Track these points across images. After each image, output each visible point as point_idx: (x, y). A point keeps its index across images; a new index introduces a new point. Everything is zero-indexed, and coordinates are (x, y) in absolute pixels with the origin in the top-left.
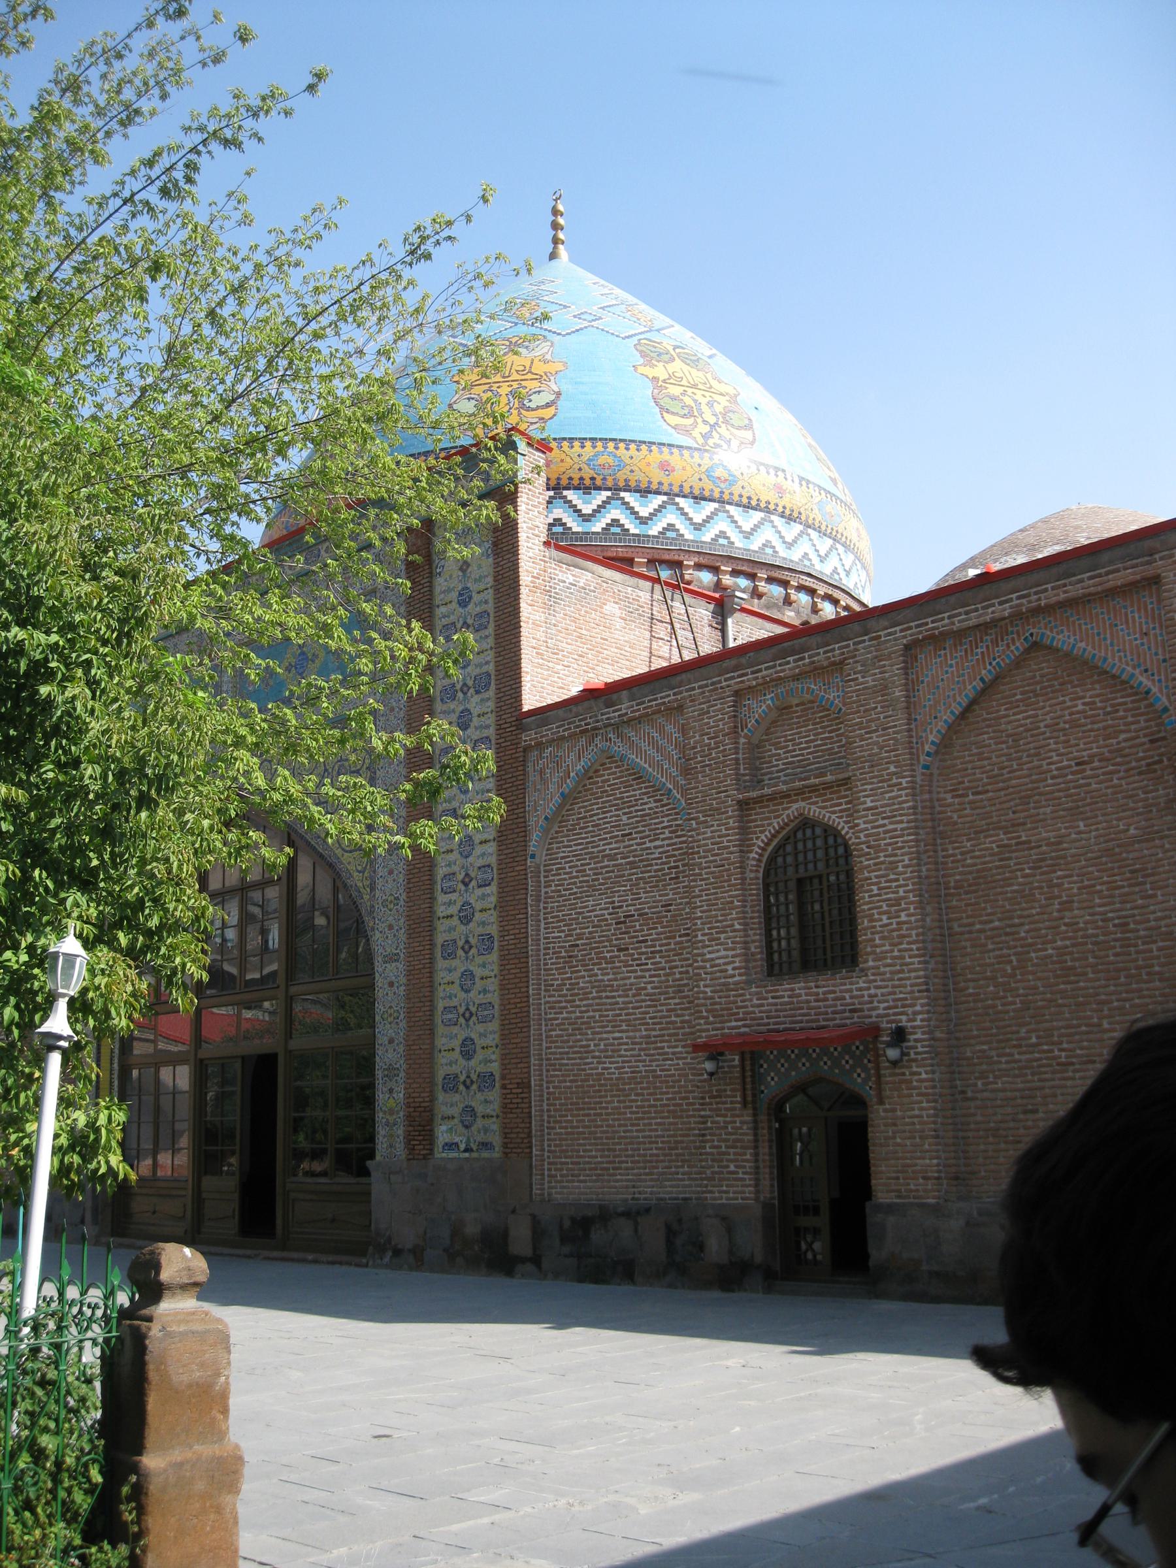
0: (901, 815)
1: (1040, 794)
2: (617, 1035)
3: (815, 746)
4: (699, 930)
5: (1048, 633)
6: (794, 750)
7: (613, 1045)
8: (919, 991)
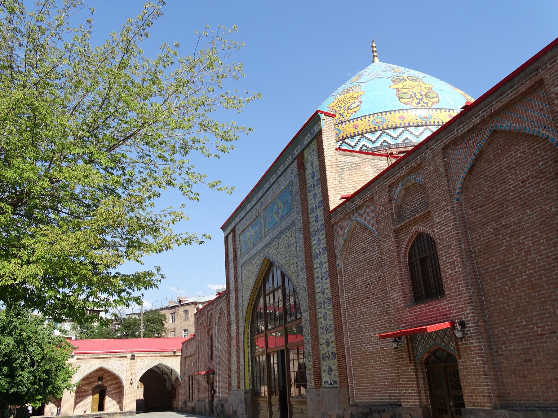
0: (450, 223)
1: (508, 201)
2: (370, 333)
3: (419, 202)
4: (387, 286)
5: (498, 124)
6: (413, 205)
7: (369, 338)
8: (467, 303)
